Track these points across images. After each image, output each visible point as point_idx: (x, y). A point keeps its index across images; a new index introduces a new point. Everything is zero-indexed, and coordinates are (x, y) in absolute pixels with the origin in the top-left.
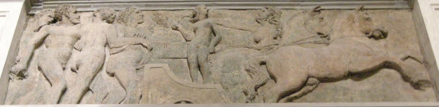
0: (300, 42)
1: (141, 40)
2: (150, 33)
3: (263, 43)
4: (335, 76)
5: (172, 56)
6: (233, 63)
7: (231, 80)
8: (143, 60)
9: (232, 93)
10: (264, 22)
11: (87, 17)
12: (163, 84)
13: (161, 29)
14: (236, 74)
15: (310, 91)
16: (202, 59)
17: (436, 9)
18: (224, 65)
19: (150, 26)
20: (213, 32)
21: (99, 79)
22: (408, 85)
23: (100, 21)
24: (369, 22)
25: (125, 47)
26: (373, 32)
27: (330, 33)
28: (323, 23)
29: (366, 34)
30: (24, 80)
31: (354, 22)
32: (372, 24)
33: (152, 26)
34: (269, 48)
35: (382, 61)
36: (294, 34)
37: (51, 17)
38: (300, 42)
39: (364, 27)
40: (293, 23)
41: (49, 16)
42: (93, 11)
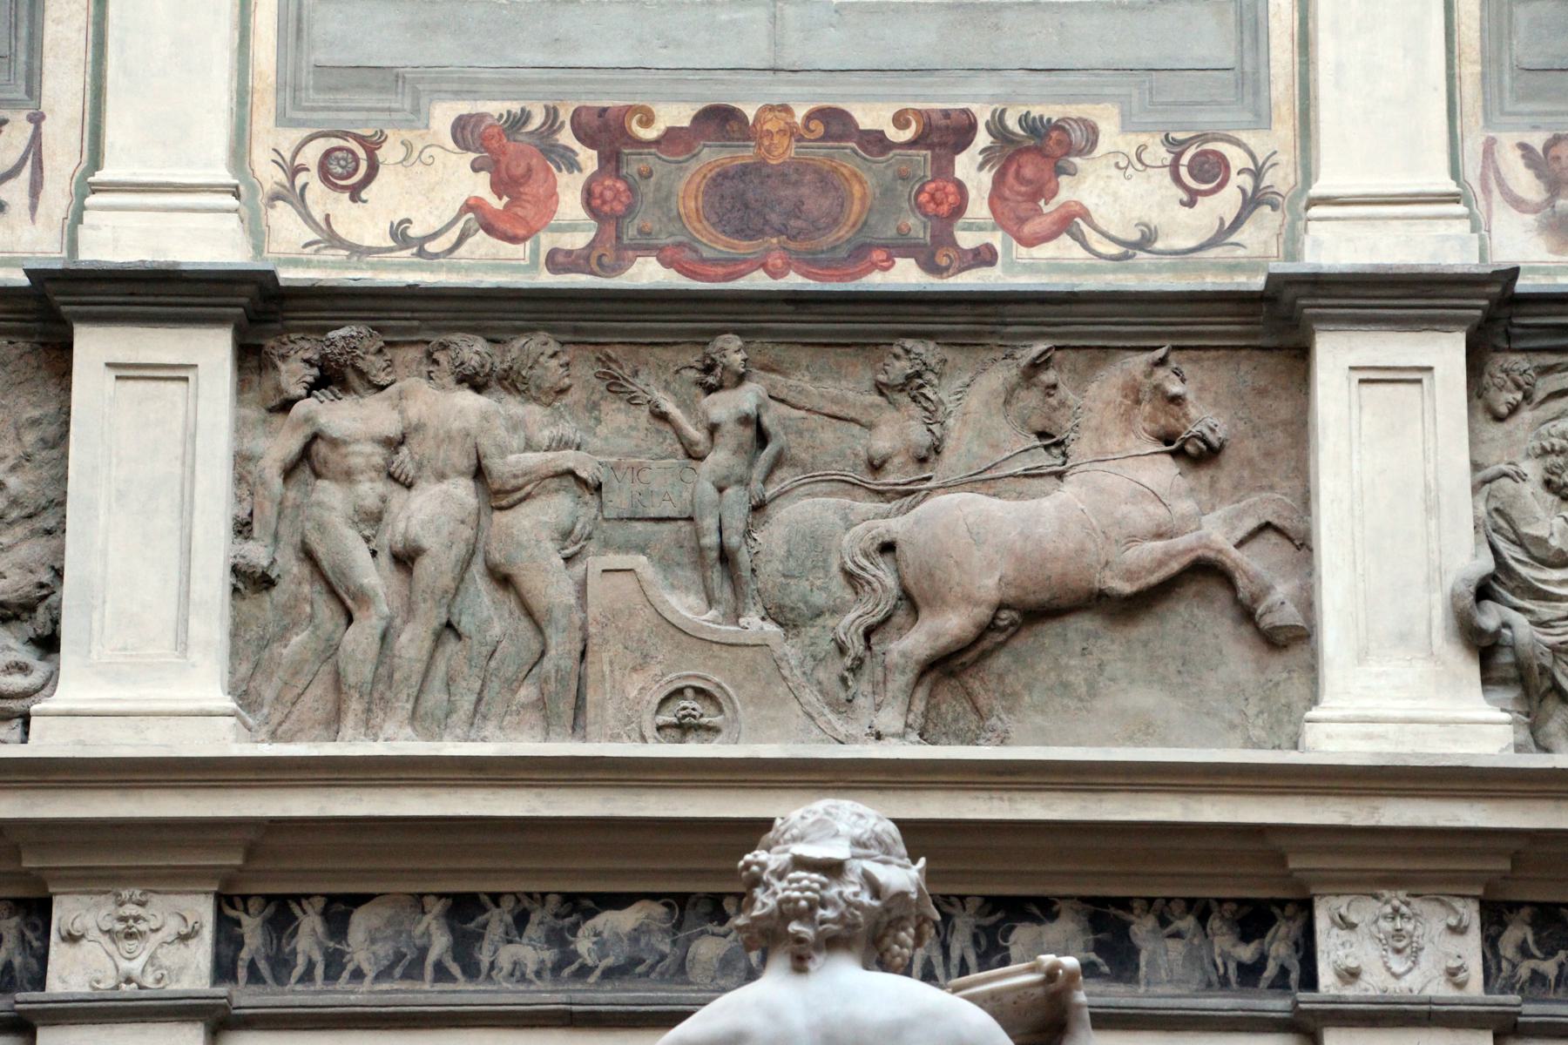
0: (987, 475)
1: (568, 459)
2: (592, 423)
3: (892, 477)
4: (1064, 603)
5: (653, 513)
6: (815, 544)
7: (806, 603)
8: (579, 526)
9: (807, 642)
10: (898, 397)
11: (413, 360)
12: (639, 627)
13: (619, 410)
14: (818, 583)
15: (1003, 644)
16: (734, 540)
17: (1361, 381)
18: (789, 553)
19: (588, 399)
20: (762, 438)
21: (472, 589)
22: (1246, 631)
23: (453, 385)
24: (1176, 409)
25: (528, 488)
26: (1186, 441)
27: (1072, 435)
28: (1053, 401)
29: (1168, 443)
30: (274, 592)
31: (1138, 402)
32: (1185, 415)
33: (596, 397)
34: (906, 494)
35: (1186, 560)
36: (975, 449)
37: (312, 365)
38: (987, 475)
39: (1163, 422)
40: (974, 401)
41: (307, 361)
42: (428, 343)
